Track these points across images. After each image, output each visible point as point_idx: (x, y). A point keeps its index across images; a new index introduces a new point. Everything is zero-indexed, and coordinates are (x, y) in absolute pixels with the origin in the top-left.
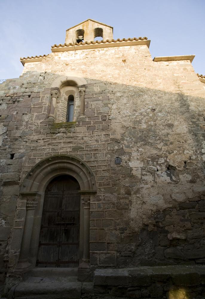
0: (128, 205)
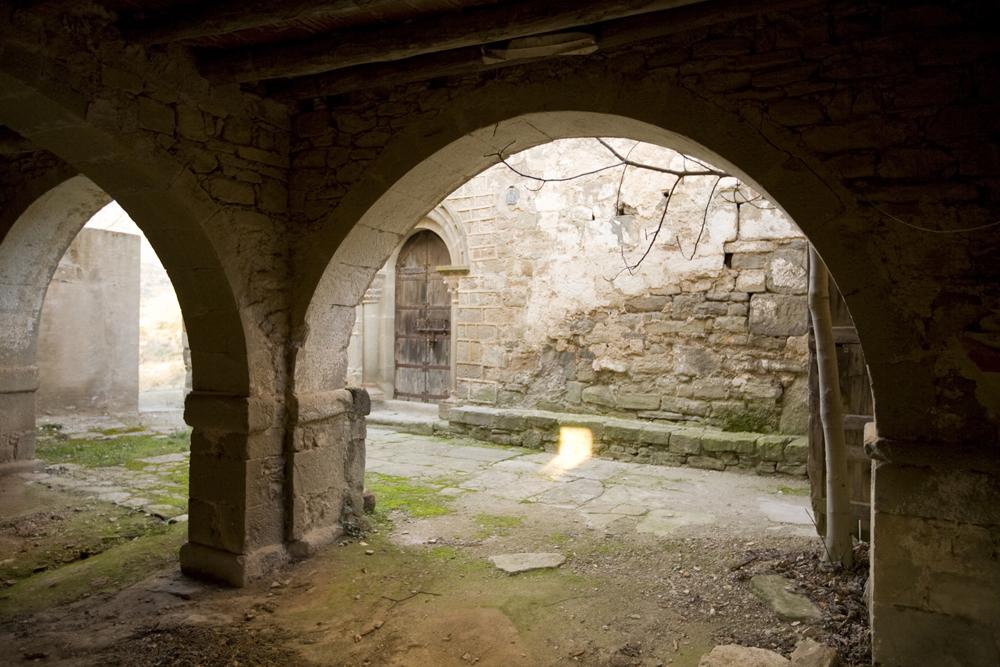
0: (524, 298)
